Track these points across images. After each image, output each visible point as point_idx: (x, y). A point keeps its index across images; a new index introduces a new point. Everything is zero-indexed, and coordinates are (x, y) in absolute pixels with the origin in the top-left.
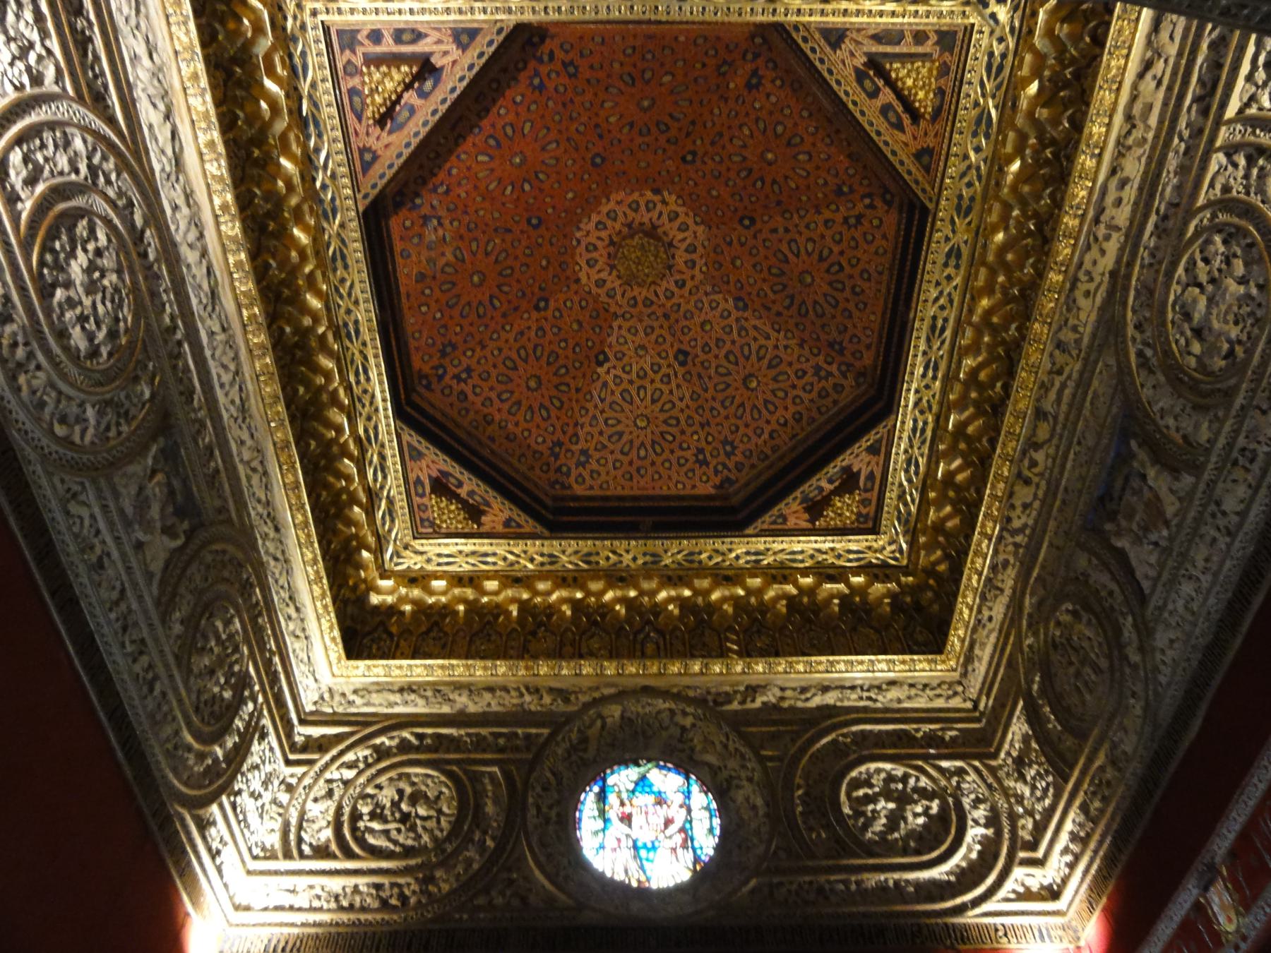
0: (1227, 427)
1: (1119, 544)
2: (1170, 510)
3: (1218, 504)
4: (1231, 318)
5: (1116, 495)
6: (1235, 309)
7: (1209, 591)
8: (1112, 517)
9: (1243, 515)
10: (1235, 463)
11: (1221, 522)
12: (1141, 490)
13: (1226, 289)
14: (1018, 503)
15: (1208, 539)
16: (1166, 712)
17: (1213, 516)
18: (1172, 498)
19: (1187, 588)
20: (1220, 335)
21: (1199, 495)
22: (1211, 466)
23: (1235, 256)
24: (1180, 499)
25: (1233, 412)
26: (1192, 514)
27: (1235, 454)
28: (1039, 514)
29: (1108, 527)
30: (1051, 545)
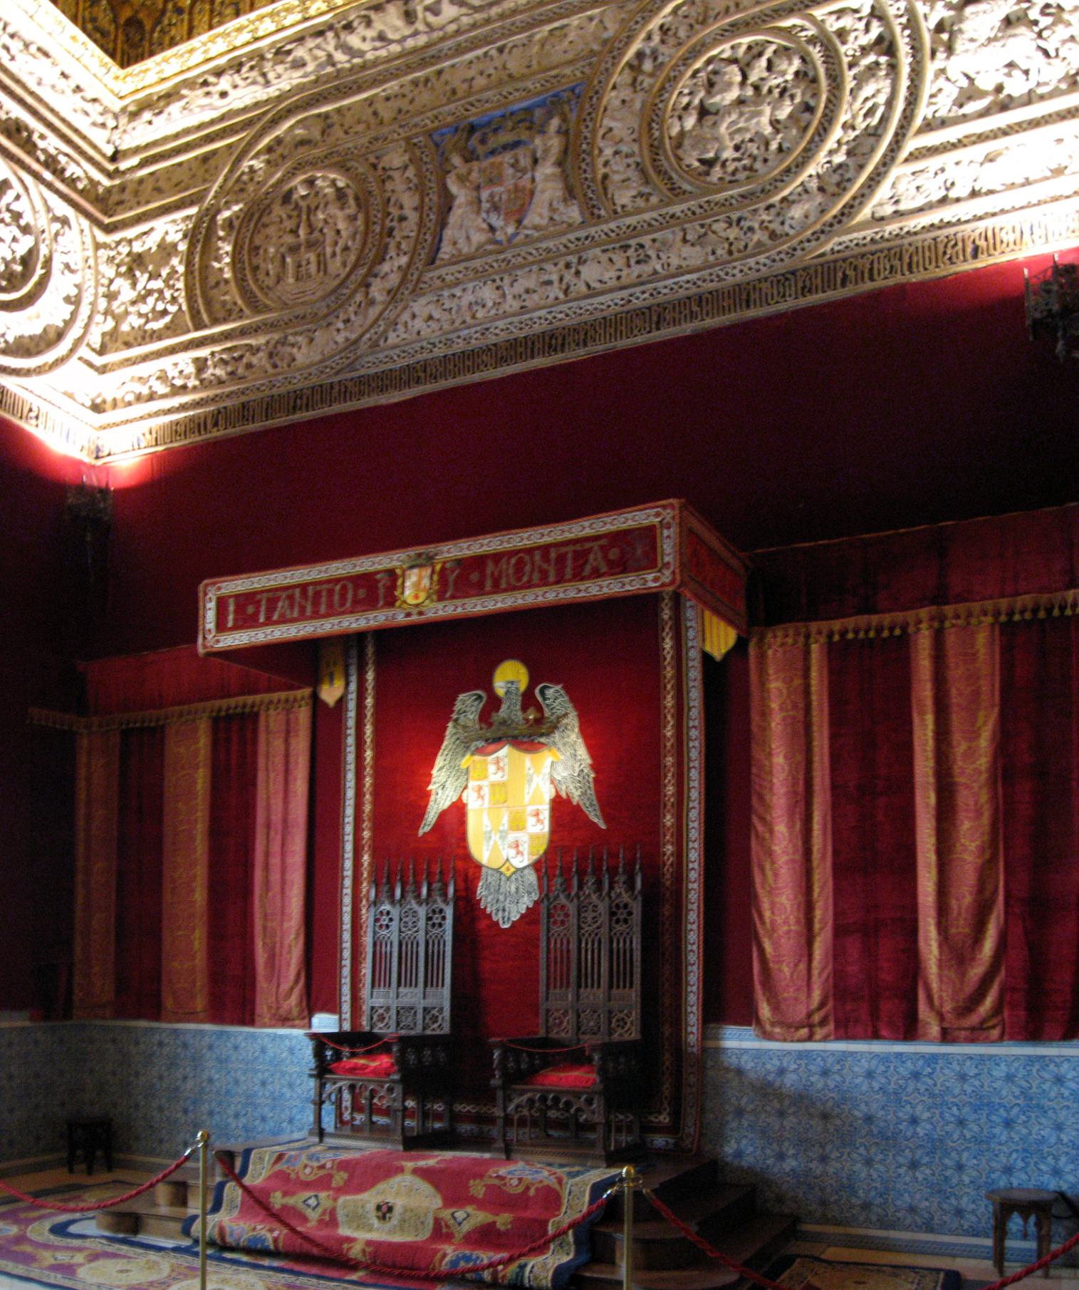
1: (454, 188)
2: (533, 218)
3: (581, 261)
5: (494, 142)
8: (470, 157)
9: (592, 293)
11: (569, 276)
12: (524, 171)
14: (378, 25)
15: (546, 278)
17: (568, 266)
18: (546, 212)
21: (572, 236)
24: (551, 219)
26: (550, 244)
28: (389, 60)
29: (456, 160)
30: (370, 102)
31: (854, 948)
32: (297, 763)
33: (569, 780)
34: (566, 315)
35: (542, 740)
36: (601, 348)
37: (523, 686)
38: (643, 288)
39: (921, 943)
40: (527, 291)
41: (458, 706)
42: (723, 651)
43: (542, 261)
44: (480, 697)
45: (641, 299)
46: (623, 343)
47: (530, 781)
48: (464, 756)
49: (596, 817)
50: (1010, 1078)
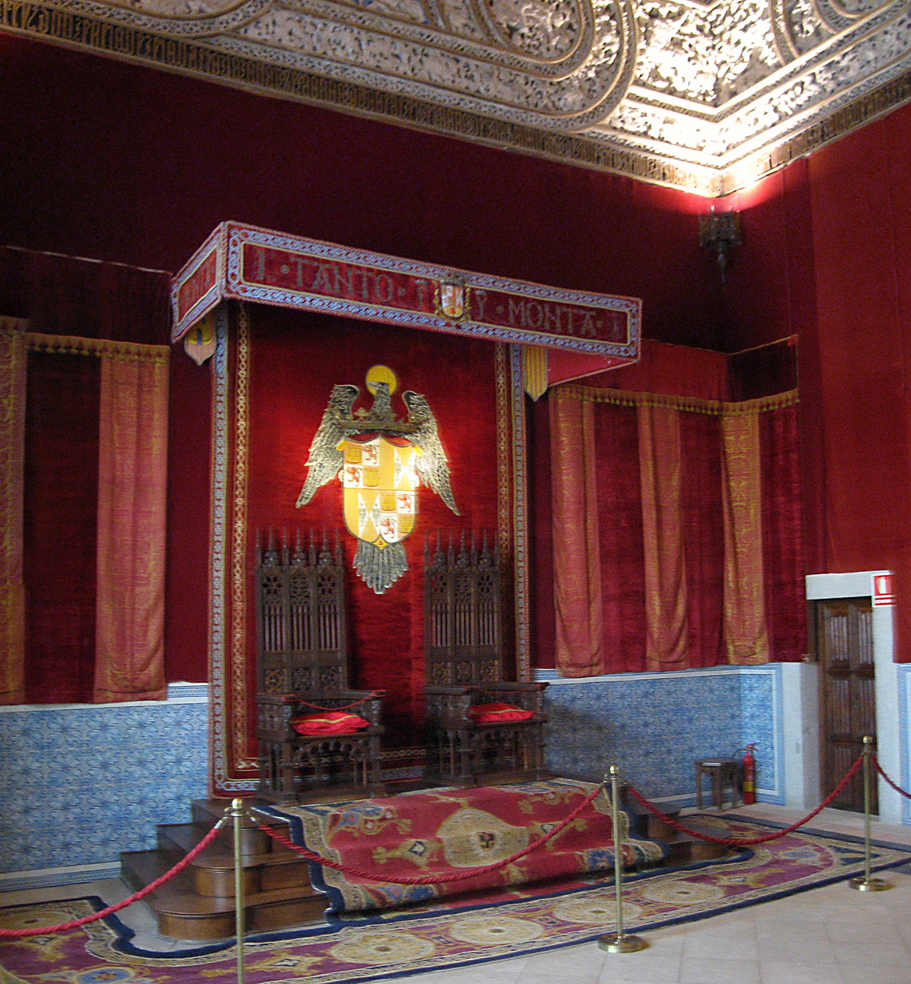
0: (473, 45)
4: (531, 23)
6: (537, 25)
7: (361, 66)
10: (458, 61)
11: (415, 60)
13: (545, 14)
16: (226, 45)
19: (347, 38)
20: (518, 15)
22: (443, 37)
23: (565, 17)
24: (398, 6)
25: (485, 48)
26: (400, 26)
27: (463, 60)
31: (613, 608)
32: (151, 419)
33: (431, 474)
34: (412, 90)
35: (407, 437)
36: (445, 131)
37: (392, 388)
38: (471, 98)
39: (648, 607)
40: (381, 55)
41: (334, 395)
42: (539, 395)
43: (397, 37)
44: (355, 392)
45: (468, 105)
46: (459, 134)
47: (399, 470)
48: (339, 440)
49: (451, 505)
50: (690, 692)
